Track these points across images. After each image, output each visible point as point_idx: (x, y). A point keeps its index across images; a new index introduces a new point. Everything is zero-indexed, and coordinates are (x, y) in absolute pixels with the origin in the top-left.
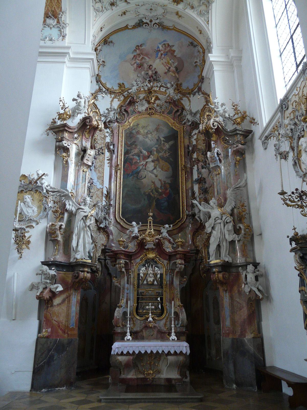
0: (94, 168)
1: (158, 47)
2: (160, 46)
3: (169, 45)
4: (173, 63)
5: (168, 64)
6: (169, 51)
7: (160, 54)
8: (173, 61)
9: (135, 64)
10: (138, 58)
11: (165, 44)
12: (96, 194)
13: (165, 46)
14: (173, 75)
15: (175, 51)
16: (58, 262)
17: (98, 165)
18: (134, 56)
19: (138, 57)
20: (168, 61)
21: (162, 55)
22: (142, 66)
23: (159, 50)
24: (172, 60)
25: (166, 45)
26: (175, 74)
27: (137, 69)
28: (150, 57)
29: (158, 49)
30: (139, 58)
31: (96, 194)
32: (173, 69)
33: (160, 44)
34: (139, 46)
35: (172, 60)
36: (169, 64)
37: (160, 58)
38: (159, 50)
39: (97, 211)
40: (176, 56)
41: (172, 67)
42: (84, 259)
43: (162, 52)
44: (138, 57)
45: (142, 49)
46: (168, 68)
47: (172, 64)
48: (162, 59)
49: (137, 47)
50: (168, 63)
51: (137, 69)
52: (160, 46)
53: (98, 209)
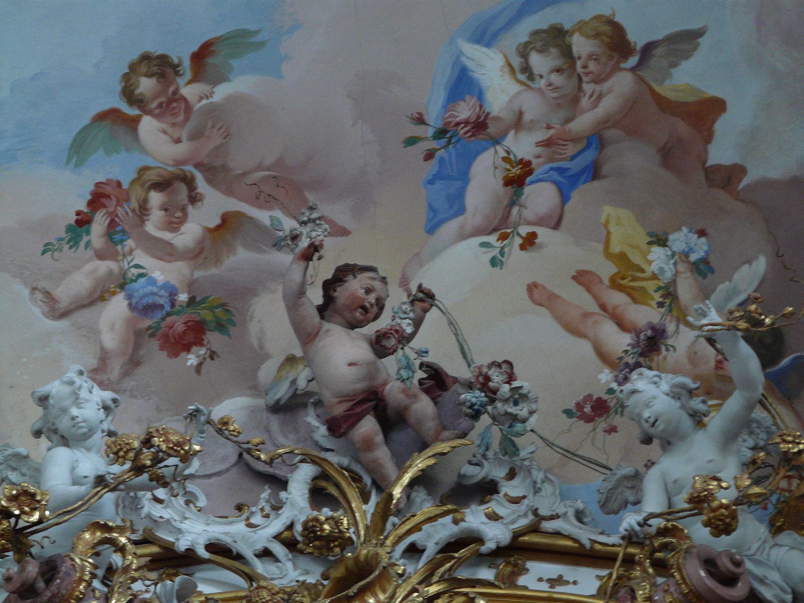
4: (702, 268)
5: (617, 299)
8: (700, 248)
9: (118, 307)
10: (151, 228)
13: (567, 53)
15: (717, 106)
18: (97, 199)
19: (156, 216)
20: (621, 258)
22: (221, 327)
23: (479, 125)
24: (680, 239)
25: (581, 45)
27: (134, 363)
29: (464, 111)
30: (174, 225)
34: (175, 68)
35: (680, 239)
36: (637, 296)
38: (479, 125)
40: (736, 172)
41: (682, 319)
44: (156, 216)
45: (213, 112)
47: (686, 290)
48: (529, 241)
49: (146, 85)
51: (134, 363)
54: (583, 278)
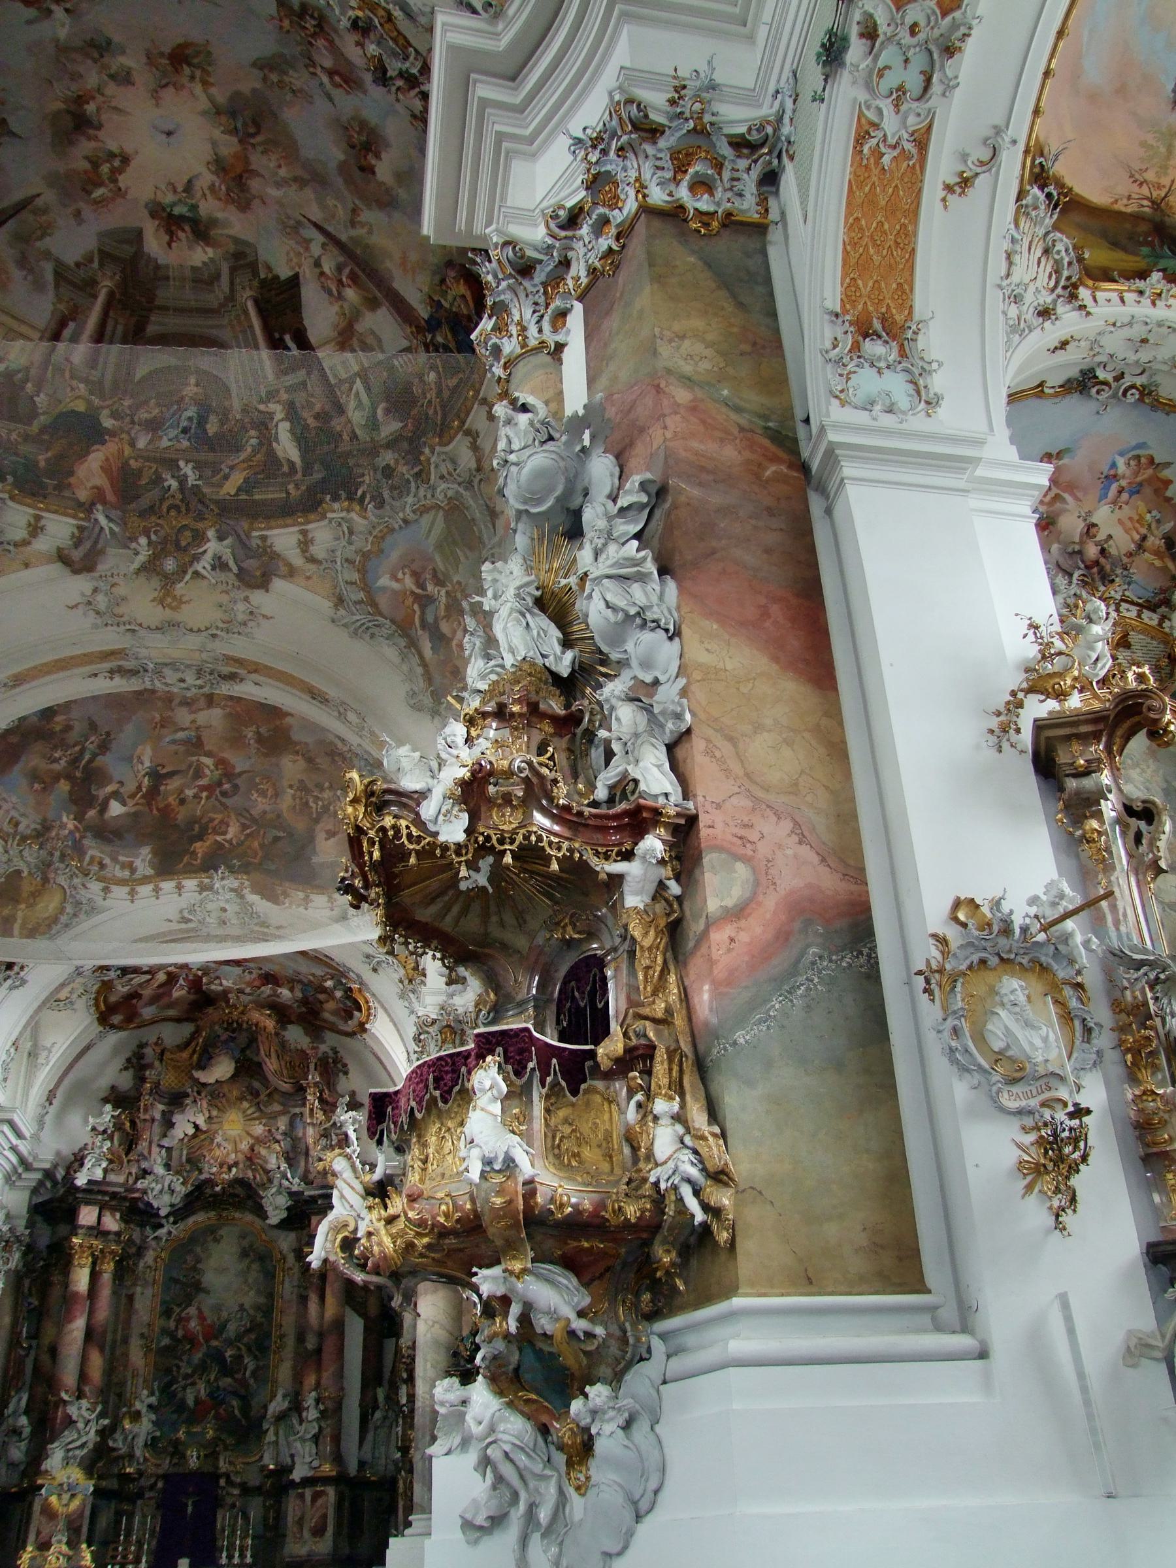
1: (1114, 465)
2: (1121, 462)
3: (1151, 460)
4: (1158, 521)
6: (1149, 481)
7: (1114, 488)
11: (1138, 457)
14: (1158, 563)
21: (1120, 492)
23: (1115, 476)
24: (1154, 513)
25: (1143, 460)
26: (1161, 558)
28: (1080, 495)
29: (1112, 472)
32: (1155, 541)
33: (1121, 454)
35: (1154, 513)
37: (1114, 502)
43: (1124, 483)
46: (1137, 537)
47: (1154, 526)
50: (1140, 520)
52: (1121, 462)
54: (1130, 519)
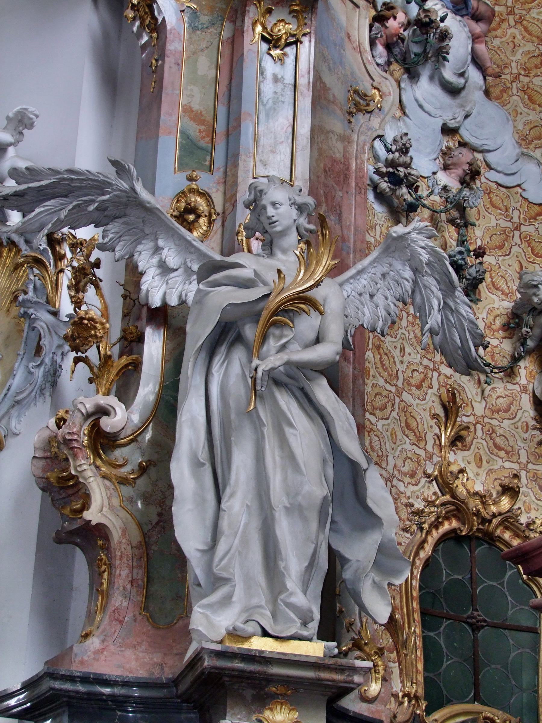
0: (474, 75)
12: (528, 240)
16: (71, 679)
17: (518, 56)
31: (528, 240)
39: (408, 286)
42: (265, 634)
53: (408, 274)
